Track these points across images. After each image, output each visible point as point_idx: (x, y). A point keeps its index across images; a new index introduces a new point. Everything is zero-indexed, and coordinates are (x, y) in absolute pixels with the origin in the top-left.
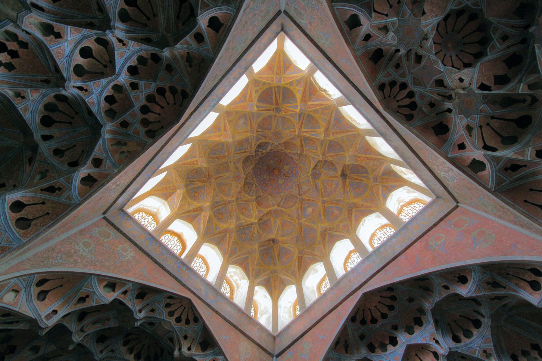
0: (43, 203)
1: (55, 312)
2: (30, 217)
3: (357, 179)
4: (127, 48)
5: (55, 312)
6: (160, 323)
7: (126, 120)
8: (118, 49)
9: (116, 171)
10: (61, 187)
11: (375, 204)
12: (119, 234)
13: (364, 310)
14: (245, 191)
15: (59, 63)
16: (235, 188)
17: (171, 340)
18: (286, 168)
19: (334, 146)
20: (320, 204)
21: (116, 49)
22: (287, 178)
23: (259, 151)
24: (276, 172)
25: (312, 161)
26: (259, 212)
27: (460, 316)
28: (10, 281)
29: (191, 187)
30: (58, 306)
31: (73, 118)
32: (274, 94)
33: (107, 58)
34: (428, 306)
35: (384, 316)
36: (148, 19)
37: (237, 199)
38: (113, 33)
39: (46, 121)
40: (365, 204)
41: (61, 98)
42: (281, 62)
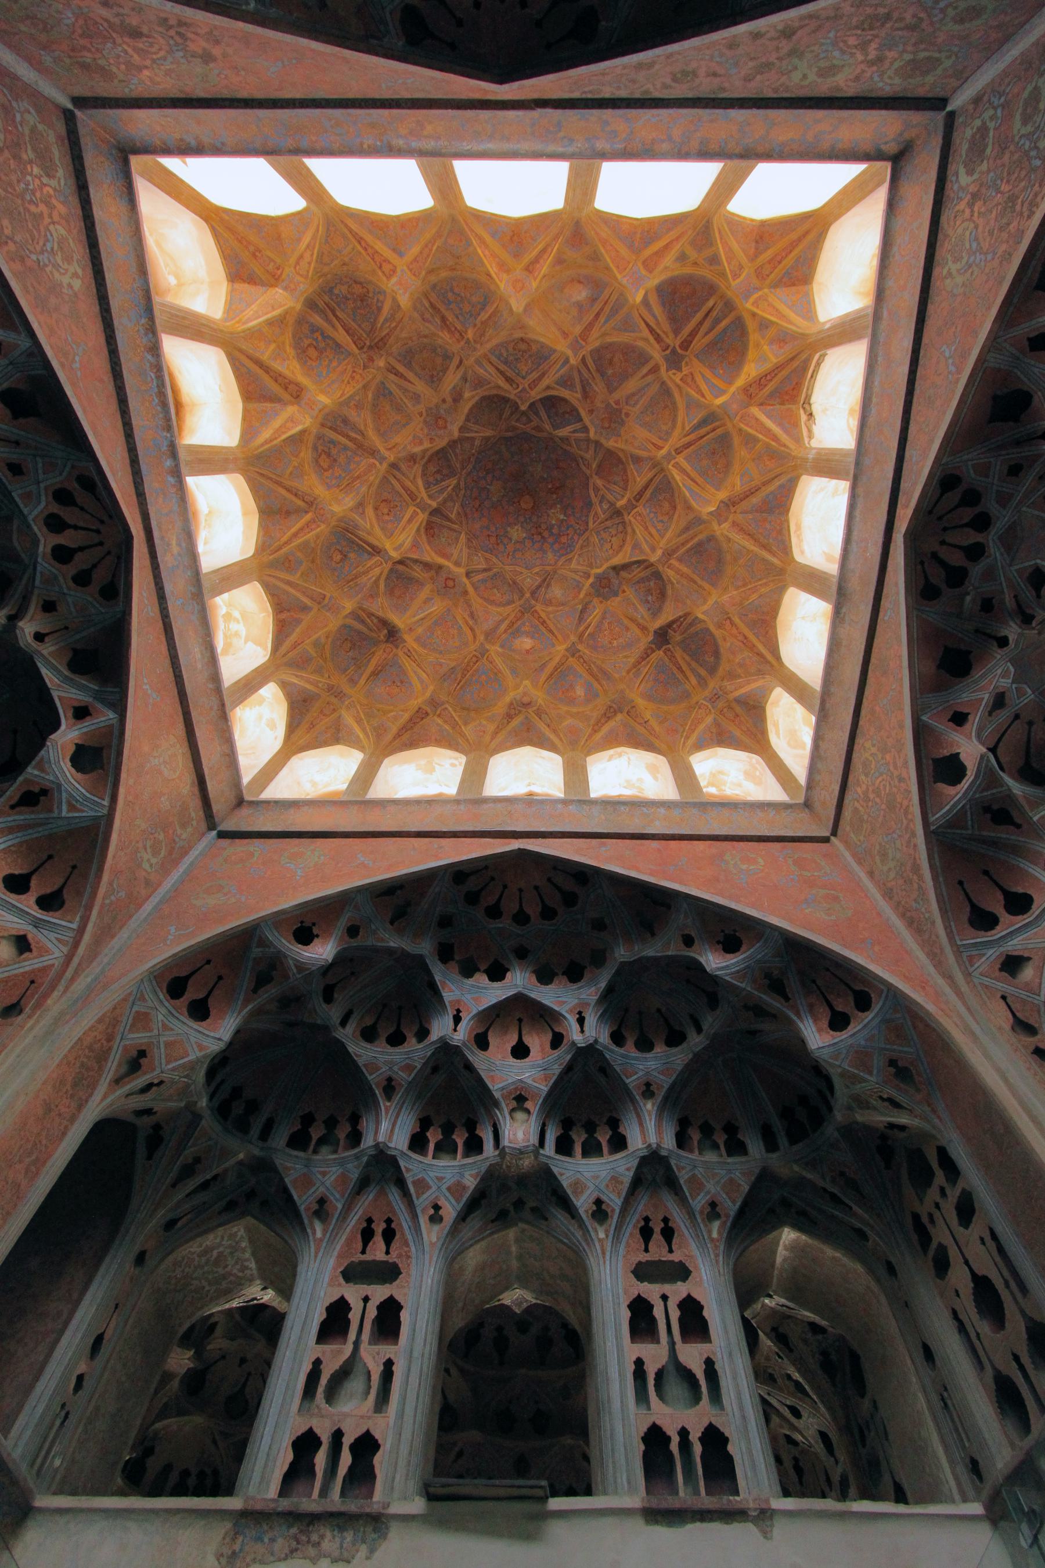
3: (680, 668)
11: (670, 742)
13: (493, 879)
14: (425, 467)
16: (411, 438)
18: (555, 515)
19: (706, 555)
20: (561, 648)
22: (537, 538)
23: (537, 414)
24: (526, 503)
25: (628, 548)
26: (415, 545)
27: (659, 1010)
29: (317, 320)
32: (710, 302)
34: (621, 954)
35: (522, 918)
37: (394, 466)
40: (654, 723)
42: (794, 246)
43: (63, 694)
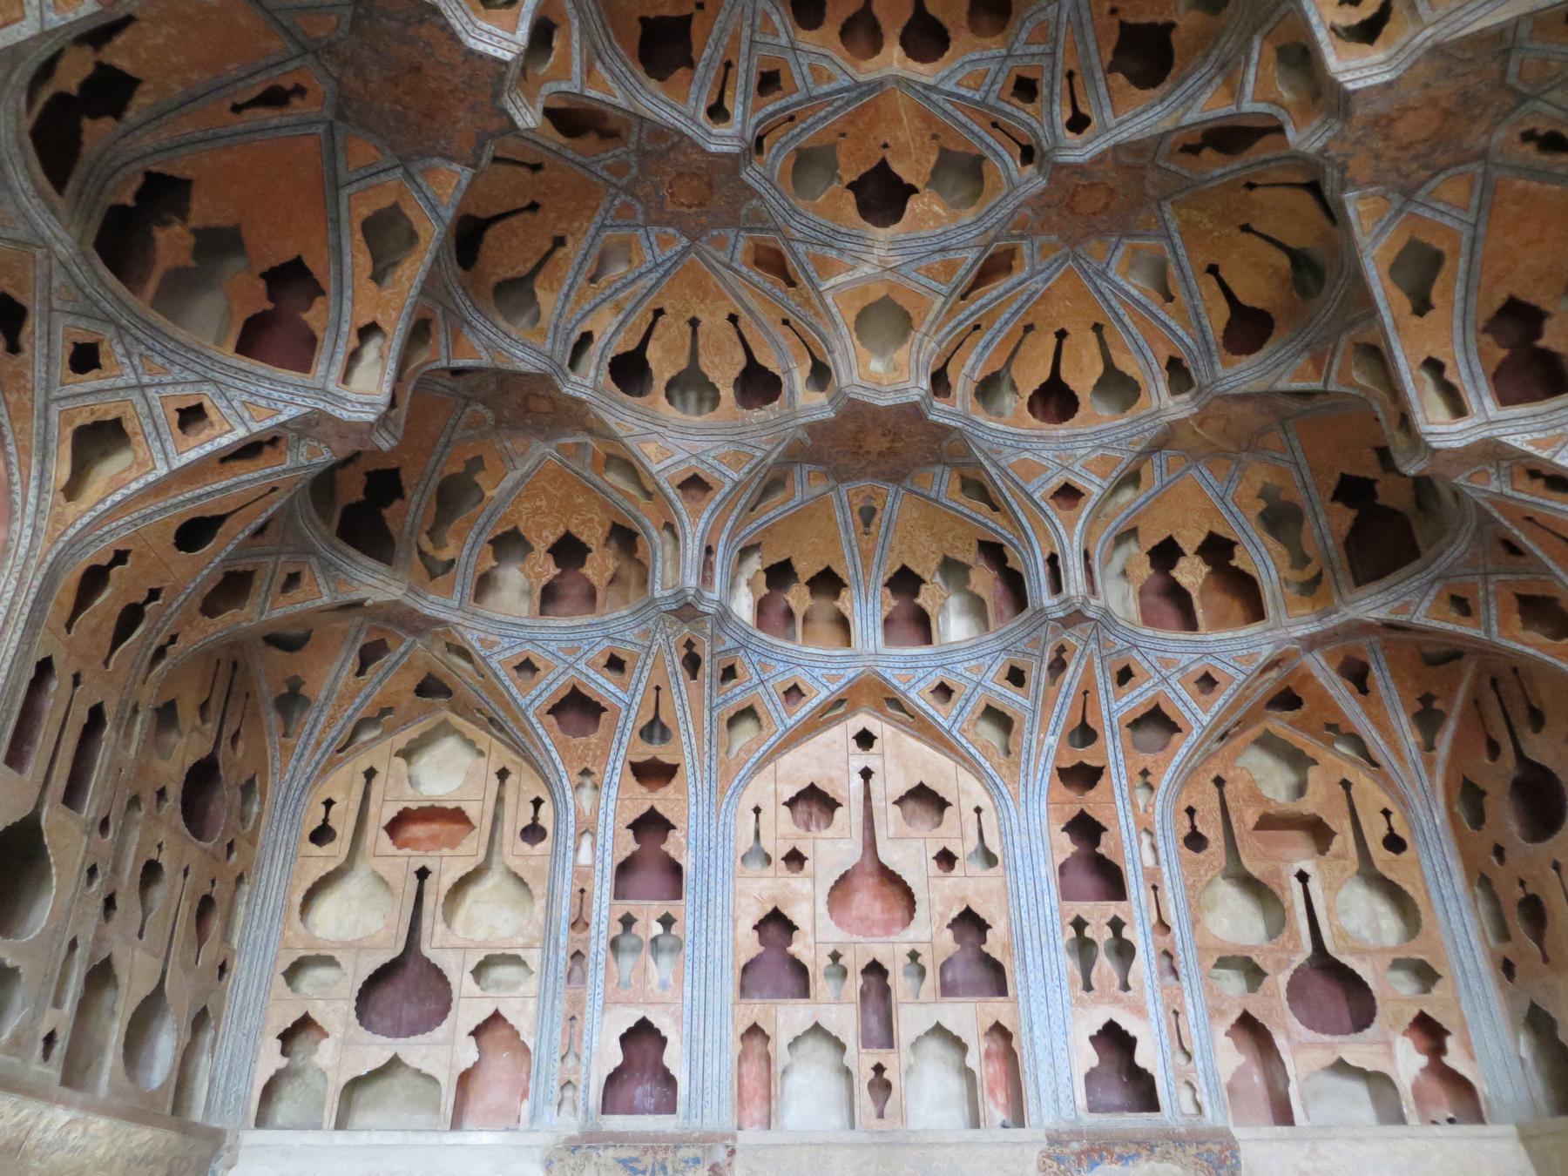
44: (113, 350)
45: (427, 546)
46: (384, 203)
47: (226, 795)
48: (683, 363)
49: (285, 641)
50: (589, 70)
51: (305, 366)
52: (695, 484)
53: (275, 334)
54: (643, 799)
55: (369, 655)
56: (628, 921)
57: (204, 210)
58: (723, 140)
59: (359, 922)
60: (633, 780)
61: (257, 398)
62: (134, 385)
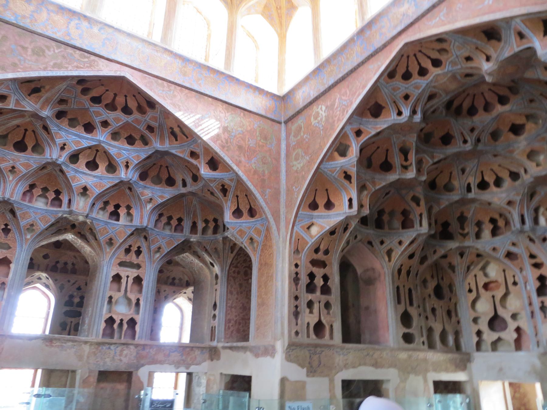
0: (237, 196)
1: (350, 200)
2: (248, 207)
4: (67, 141)
5: (350, 200)
6: (434, 87)
7: (145, 128)
8: (73, 148)
9: (199, 141)
10: (220, 185)
12: (303, 113)
15: (108, 186)
17: (468, 75)
21: (73, 149)
28: (295, 231)
30: (347, 195)
31: (161, 166)
33: (88, 151)
36: (26, 130)
38: (57, 160)
39: (171, 182)
41: (143, 176)
43: (515, 46)
44: (385, 239)
45: (461, 231)
46: (412, 195)
47: (446, 291)
48: (495, 177)
49: (445, 256)
50: (432, 157)
51: (413, 227)
52: (510, 203)
53: (406, 224)
54: (538, 273)
55: (462, 255)
56: (542, 302)
57: (387, 210)
58: (468, 147)
59: (484, 308)
60: (533, 268)
61: (408, 236)
62: (391, 242)
